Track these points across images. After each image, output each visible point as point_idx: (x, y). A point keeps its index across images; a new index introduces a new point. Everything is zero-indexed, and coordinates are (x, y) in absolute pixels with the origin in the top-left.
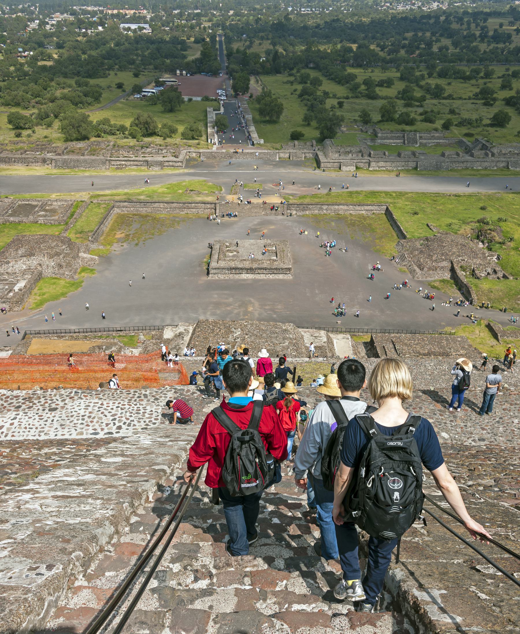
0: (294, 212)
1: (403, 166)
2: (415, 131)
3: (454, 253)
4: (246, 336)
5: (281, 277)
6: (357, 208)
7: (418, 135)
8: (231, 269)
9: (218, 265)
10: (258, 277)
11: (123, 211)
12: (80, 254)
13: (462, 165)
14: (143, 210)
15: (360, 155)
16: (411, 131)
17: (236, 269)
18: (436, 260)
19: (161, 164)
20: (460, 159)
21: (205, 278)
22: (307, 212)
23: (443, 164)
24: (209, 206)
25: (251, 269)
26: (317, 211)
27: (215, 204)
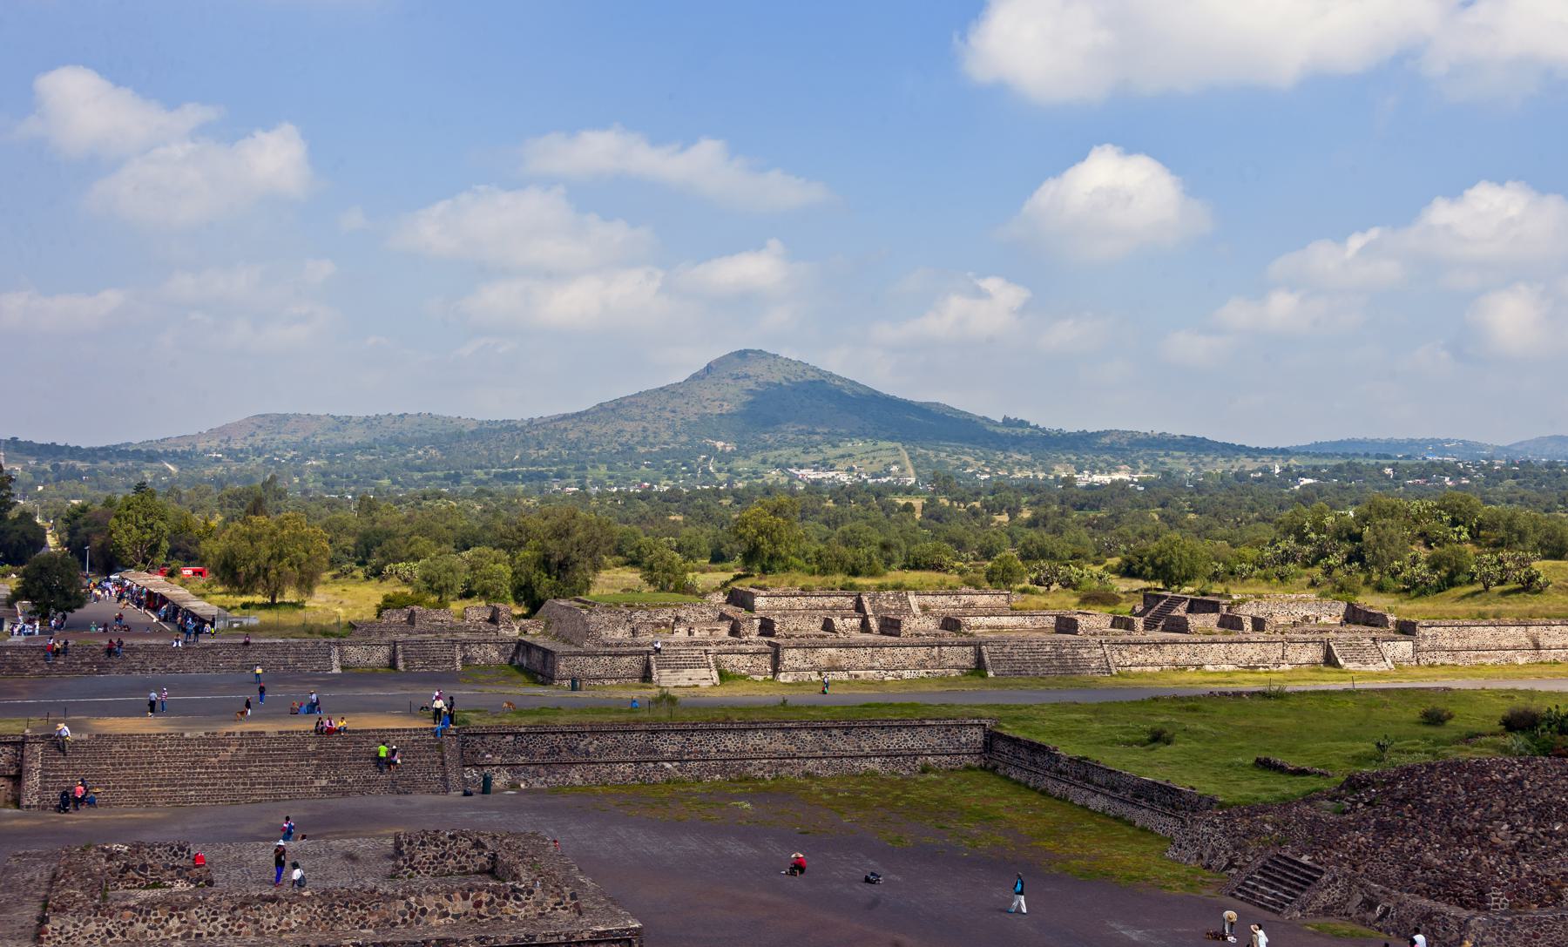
0: (500, 780)
1: (922, 665)
2: (898, 587)
6: (840, 743)
7: (913, 599)
13: (1155, 655)
15: (724, 630)
18: (1521, 845)
20: (1135, 636)
22: (576, 776)
26: (628, 769)
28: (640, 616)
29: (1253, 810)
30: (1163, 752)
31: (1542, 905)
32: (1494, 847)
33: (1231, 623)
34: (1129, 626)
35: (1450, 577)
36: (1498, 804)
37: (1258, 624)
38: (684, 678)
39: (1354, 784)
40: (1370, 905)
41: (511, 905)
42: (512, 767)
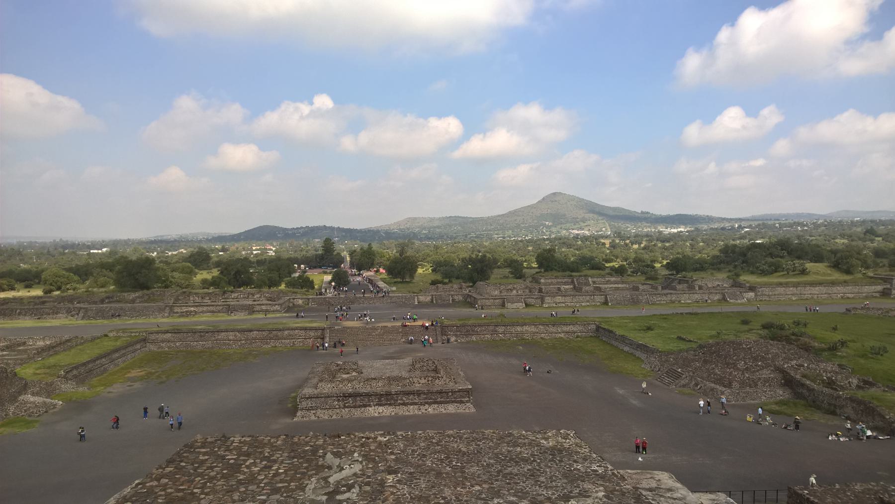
0: (453, 339)
1: (588, 301)
2: (585, 276)
3: (776, 356)
4: (390, 479)
5: (451, 408)
6: (552, 329)
7: (590, 279)
8: (346, 396)
9: (316, 392)
10: (402, 411)
11: (162, 347)
12: (21, 398)
14: (198, 345)
15: (527, 291)
16: (580, 276)
17: (355, 395)
18: (747, 369)
19: (251, 310)
20: (659, 292)
21: (288, 420)
22: (474, 338)
23: (640, 297)
24: (312, 334)
25: (388, 394)
27: (323, 329)
28: (502, 287)
29: (669, 353)
30: (650, 333)
31: (751, 387)
32: (738, 369)
33: (691, 288)
34: (656, 289)
35: (775, 269)
36: (742, 355)
37: (700, 288)
38: (515, 305)
39: (701, 347)
40: (697, 385)
41: (437, 381)
42: (456, 336)
